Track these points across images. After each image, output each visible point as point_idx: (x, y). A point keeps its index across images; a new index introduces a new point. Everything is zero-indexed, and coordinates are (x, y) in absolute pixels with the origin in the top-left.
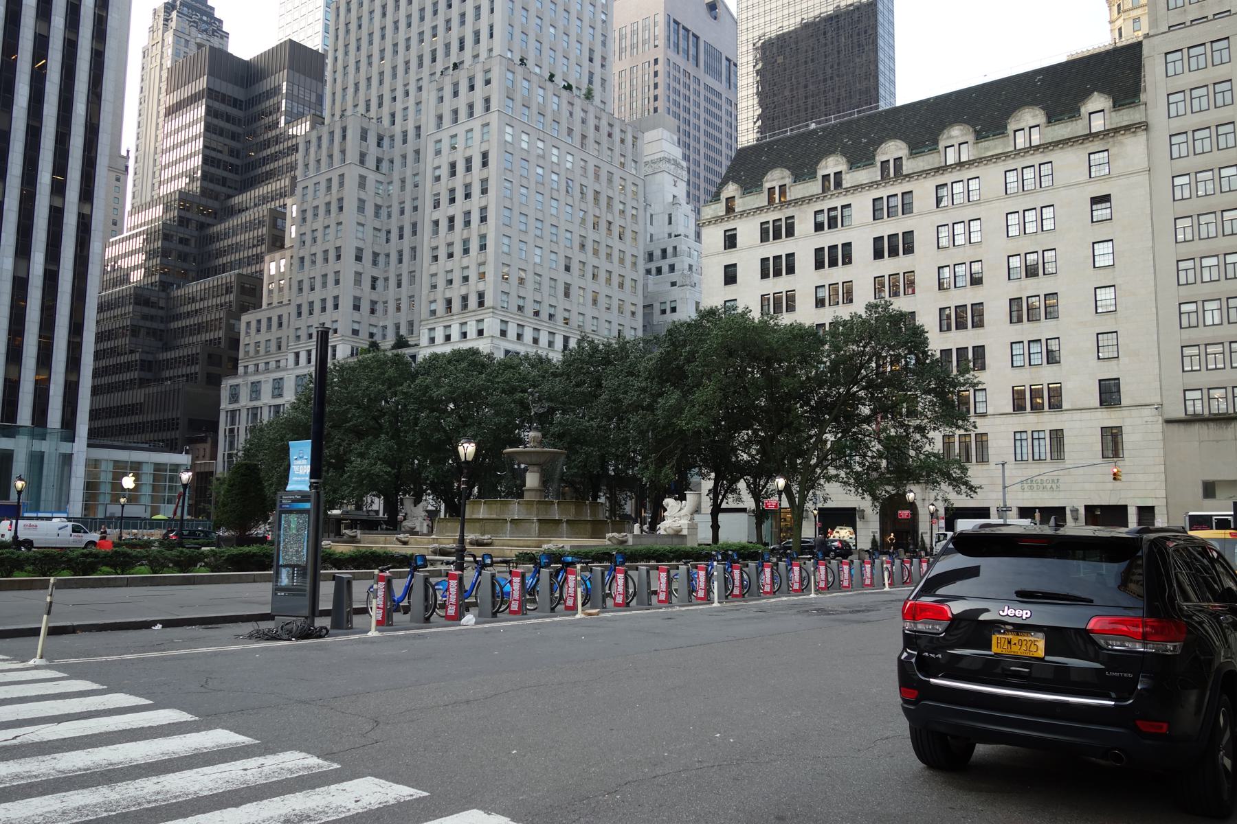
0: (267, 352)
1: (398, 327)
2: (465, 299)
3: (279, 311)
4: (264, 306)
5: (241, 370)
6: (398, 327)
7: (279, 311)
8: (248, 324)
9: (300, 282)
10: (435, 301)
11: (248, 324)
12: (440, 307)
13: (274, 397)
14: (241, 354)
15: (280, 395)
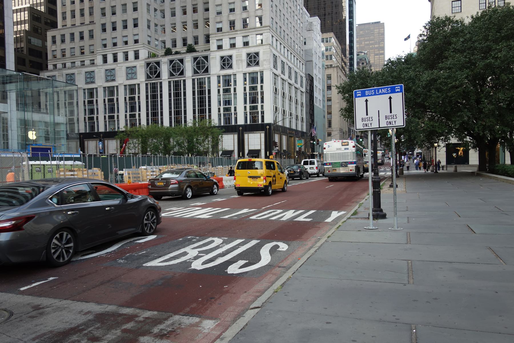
0: (73, 55)
1: (185, 40)
2: (63, 41)
3: (81, 29)
4: (60, 26)
5: (50, 67)
6: (185, 40)
7: (81, 29)
8: (54, 37)
9: (103, 9)
10: (221, 22)
11: (54, 37)
12: (226, 27)
13: (87, 83)
14: (50, 57)
15: (93, 82)
